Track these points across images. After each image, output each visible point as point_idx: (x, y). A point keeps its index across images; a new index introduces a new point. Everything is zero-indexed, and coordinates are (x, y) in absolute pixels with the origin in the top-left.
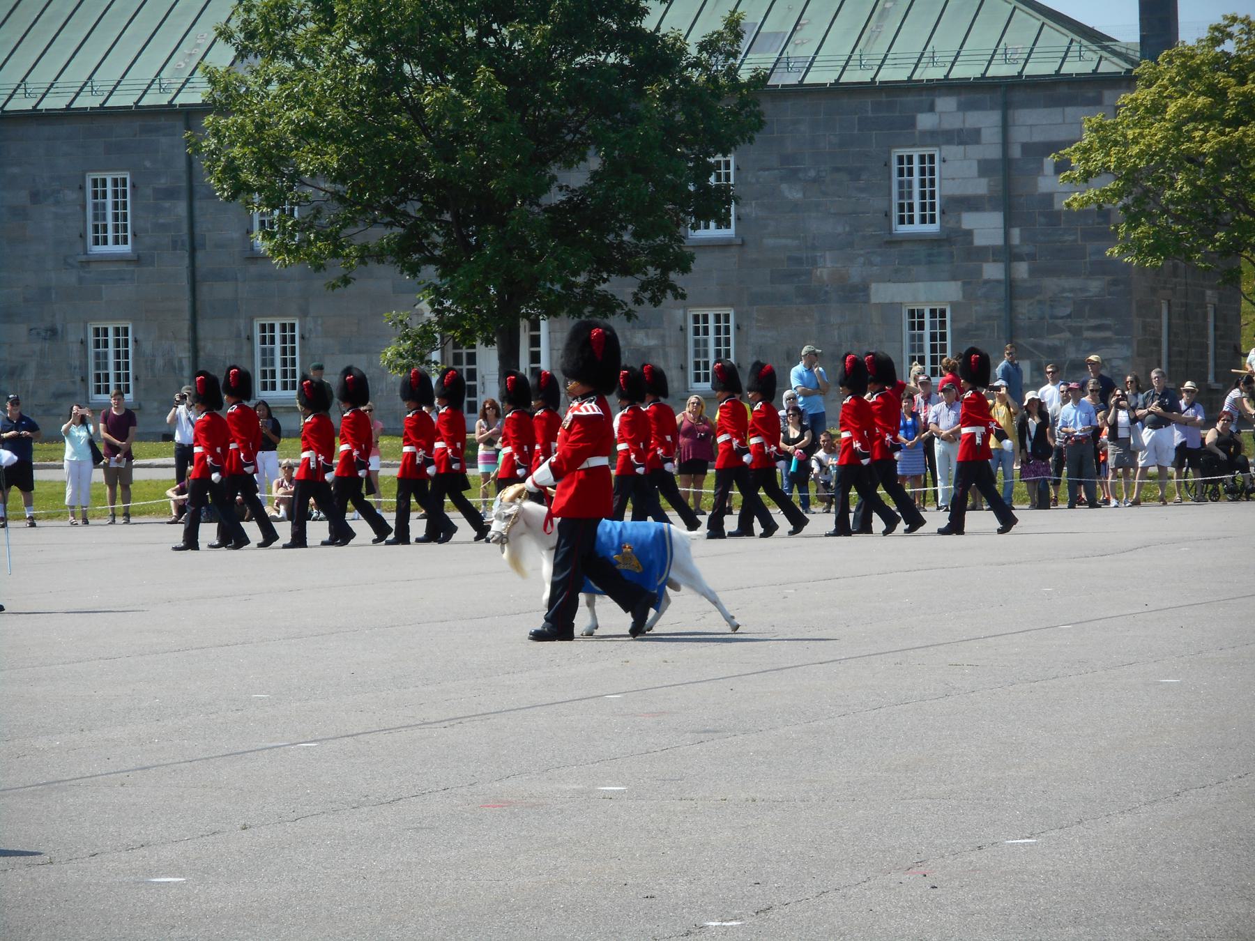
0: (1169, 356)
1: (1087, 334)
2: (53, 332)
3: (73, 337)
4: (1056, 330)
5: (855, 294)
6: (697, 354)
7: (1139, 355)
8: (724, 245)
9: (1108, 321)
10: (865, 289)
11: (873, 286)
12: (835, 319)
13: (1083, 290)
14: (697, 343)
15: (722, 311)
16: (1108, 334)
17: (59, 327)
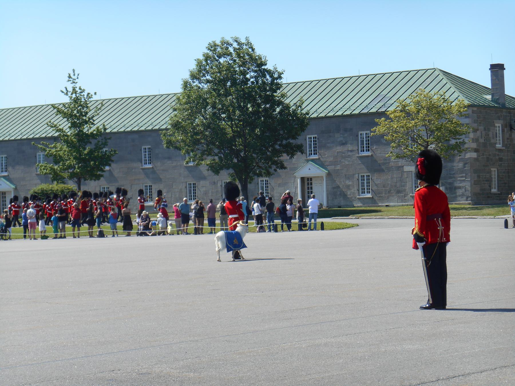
0: (498, 184)
1: (459, 179)
2: (214, 183)
3: (219, 184)
4: (451, 178)
5: (400, 168)
6: (362, 186)
7: (475, 184)
8: (368, 156)
9: (464, 175)
10: (403, 166)
11: (405, 167)
12: (395, 176)
13: (458, 166)
14: (362, 183)
15: (368, 174)
16: (464, 179)
17: (216, 181)
